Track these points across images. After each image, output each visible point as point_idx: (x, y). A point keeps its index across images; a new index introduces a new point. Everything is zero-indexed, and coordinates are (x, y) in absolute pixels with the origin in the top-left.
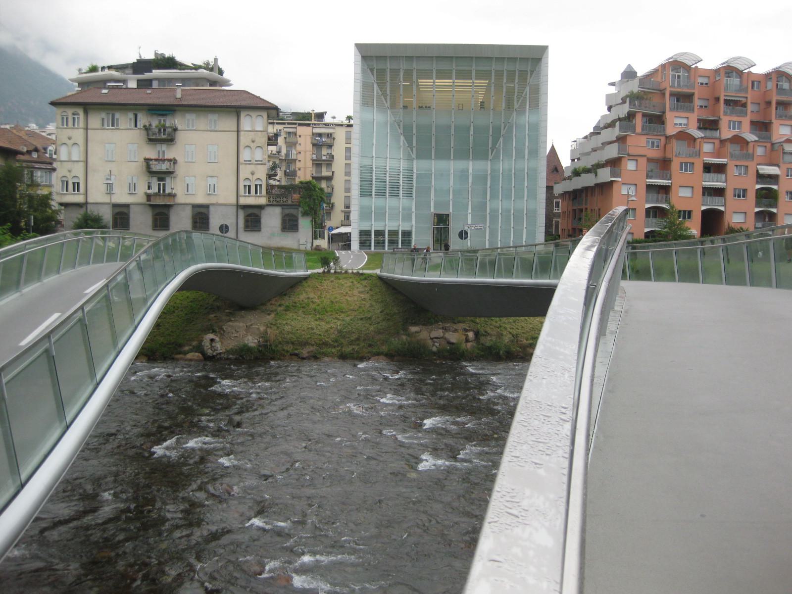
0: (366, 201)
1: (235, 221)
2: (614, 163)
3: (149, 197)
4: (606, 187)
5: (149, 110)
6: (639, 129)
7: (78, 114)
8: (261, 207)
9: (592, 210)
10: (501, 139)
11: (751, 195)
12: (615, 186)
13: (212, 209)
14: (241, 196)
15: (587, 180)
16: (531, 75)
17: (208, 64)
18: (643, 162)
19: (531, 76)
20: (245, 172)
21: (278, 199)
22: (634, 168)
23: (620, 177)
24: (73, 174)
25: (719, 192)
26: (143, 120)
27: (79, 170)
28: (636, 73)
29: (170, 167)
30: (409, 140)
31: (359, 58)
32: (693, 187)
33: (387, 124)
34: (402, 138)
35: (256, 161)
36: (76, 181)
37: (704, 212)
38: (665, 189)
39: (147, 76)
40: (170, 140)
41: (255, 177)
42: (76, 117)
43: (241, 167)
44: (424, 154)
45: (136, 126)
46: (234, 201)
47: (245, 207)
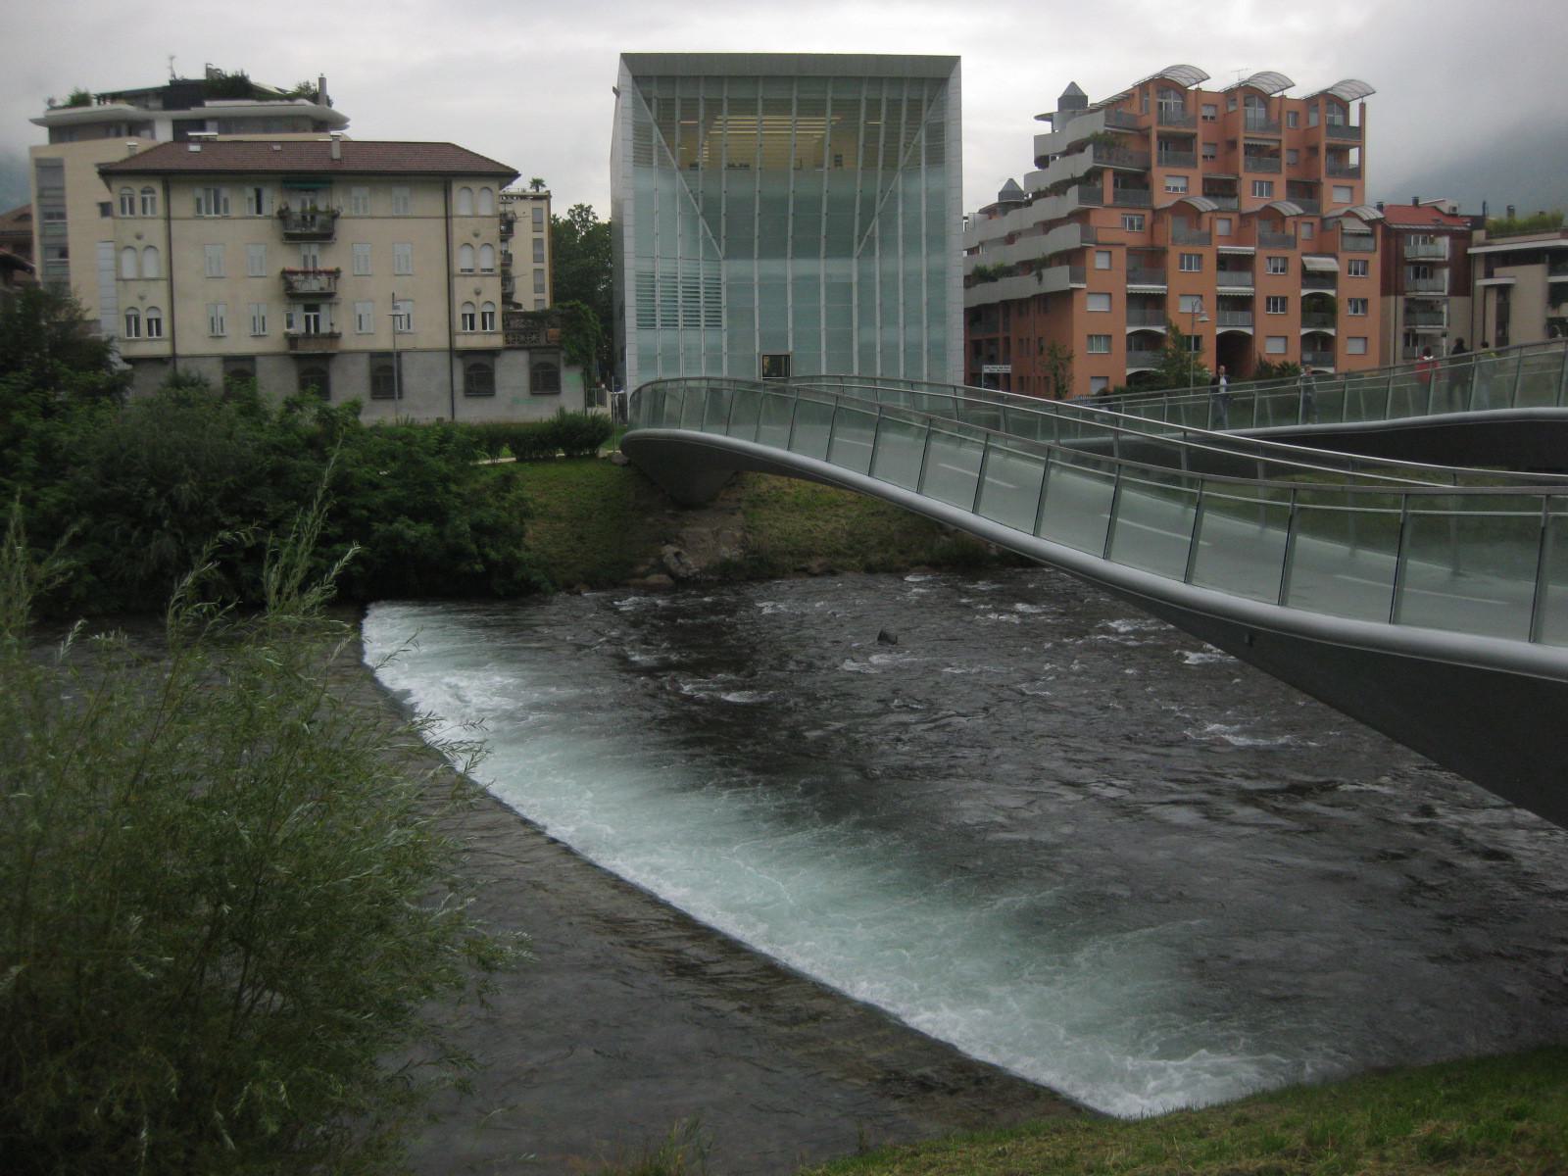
0: (648, 336)
1: (447, 378)
2: (1071, 258)
3: (292, 340)
4: (1067, 295)
5: (285, 182)
6: (1108, 198)
7: (153, 192)
8: (493, 353)
9: (1021, 340)
10: (876, 222)
11: (1295, 307)
12: (1076, 297)
13: (405, 357)
14: (459, 334)
15: (1023, 287)
16: (929, 106)
17: (307, 87)
18: (1120, 254)
19: (929, 106)
20: (464, 289)
21: (522, 338)
22: (1106, 266)
23: (1084, 282)
24: (149, 303)
25: (1242, 303)
26: (273, 202)
27: (158, 295)
28: (1085, 98)
29: (329, 285)
30: (714, 224)
31: (629, 79)
32: (1201, 296)
33: (675, 196)
34: (702, 221)
35: (483, 270)
36: (154, 315)
37: (1221, 339)
38: (1157, 301)
39: (194, 112)
40: (325, 236)
41: (482, 299)
42: (148, 196)
43: (457, 282)
44: (738, 249)
45: (259, 211)
46: (446, 345)
47: (466, 353)
